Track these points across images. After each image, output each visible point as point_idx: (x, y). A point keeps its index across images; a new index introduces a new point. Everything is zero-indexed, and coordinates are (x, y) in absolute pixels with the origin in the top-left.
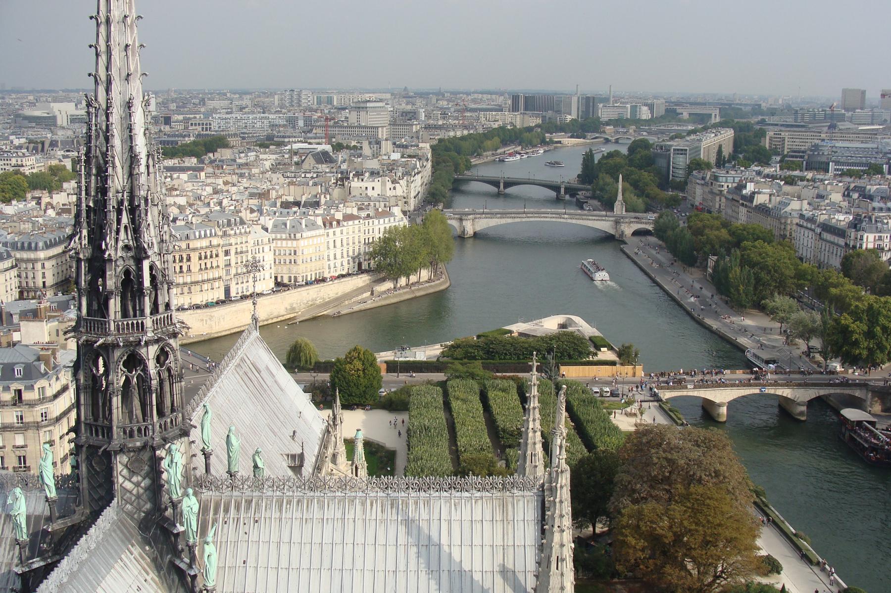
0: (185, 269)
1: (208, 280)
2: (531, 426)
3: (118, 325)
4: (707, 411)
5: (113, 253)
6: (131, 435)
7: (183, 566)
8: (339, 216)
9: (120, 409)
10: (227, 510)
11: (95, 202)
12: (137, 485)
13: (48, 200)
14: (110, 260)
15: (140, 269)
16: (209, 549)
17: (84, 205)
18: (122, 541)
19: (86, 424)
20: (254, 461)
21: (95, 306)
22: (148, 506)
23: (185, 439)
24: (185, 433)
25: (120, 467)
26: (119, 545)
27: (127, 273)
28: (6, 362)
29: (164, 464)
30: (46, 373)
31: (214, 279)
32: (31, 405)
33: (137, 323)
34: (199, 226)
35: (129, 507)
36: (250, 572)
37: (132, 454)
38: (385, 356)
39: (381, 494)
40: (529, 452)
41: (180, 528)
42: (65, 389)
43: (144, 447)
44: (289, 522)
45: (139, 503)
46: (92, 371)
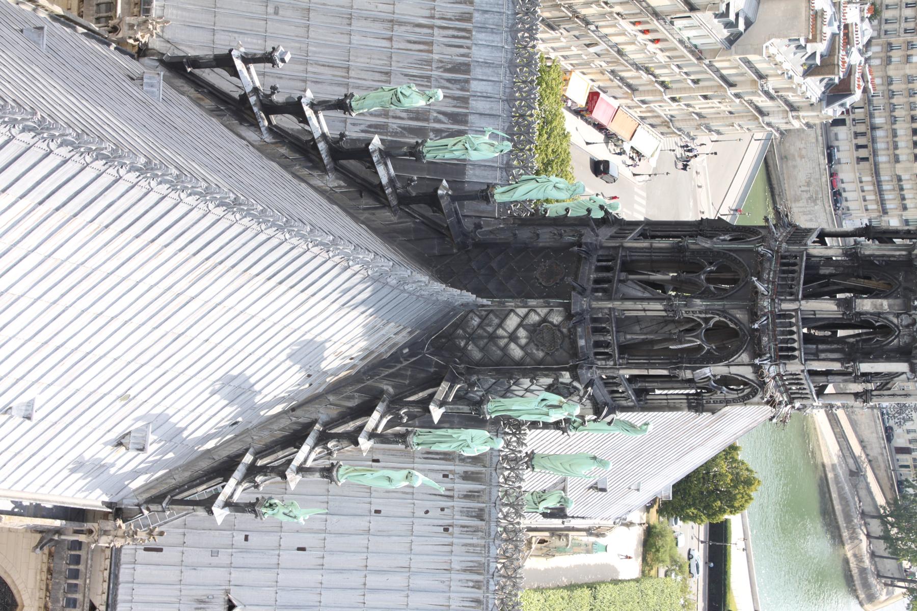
3: (791, 317)
6: (596, 330)
9: (642, 313)
10: (466, 477)
12: (513, 337)
21: (824, 271)
22: (477, 355)
25: (543, 311)
27: (886, 330)
33: (794, 349)
35: (476, 321)
36: (362, 523)
37: (565, 330)
41: (437, 413)
43: (574, 352)
44: (443, 587)
45: (481, 337)
46: (711, 264)
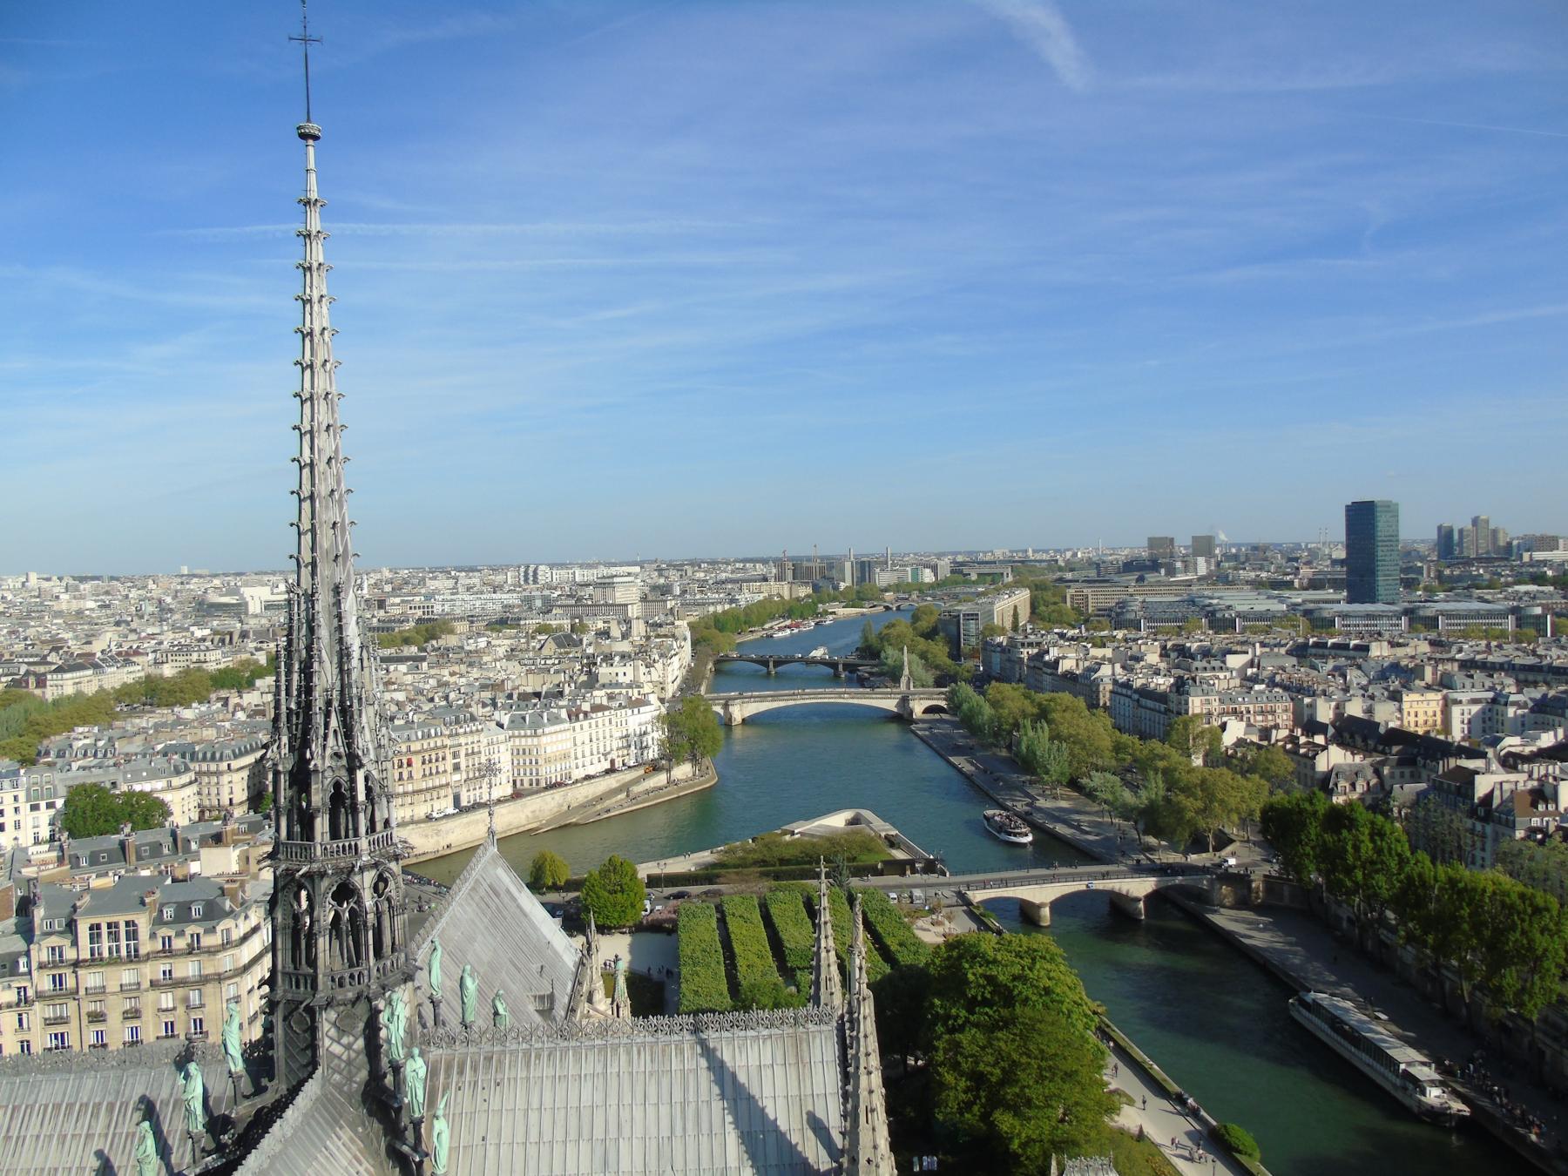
0: (405, 776)
1: (434, 788)
2: (823, 944)
4: (1026, 915)
5: (319, 763)
6: (341, 985)
7: (405, 1149)
8: (586, 707)
10: (461, 1072)
11: (298, 704)
12: (348, 1047)
13: (237, 700)
14: (316, 771)
15: (353, 781)
16: (440, 1125)
17: (283, 708)
18: (328, 1123)
19: (284, 974)
20: (495, 1007)
23: (410, 984)
24: (408, 978)
25: (326, 1026)
26: (323, 1129)
27: (337, 785)
28: (181, 900)
29: (383, 1018)
30: (232, 911)
31: (441, 786)
32: (212, 951)
34: (422, 725)
35: (337, 1077)
36: (491, 1151)
38: (645, 870)
39: (649, 1039)
40: (823, 976)
42: (255, 930)
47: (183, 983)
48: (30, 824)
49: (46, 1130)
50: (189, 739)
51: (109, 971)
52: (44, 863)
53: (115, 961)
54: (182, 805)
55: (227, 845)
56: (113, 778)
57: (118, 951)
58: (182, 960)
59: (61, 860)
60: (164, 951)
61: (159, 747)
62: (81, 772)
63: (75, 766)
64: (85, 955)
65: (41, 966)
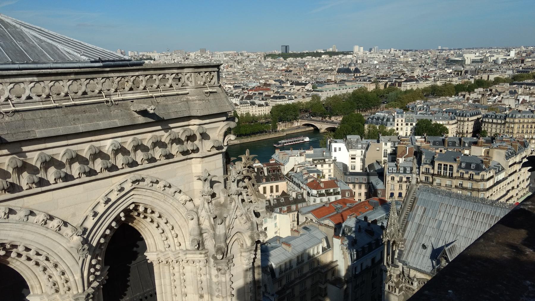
13: (468, 96)
28: (468, 161)
47: (466, 189)
48: (405, 129)
49: (485, 221)
50: (454, 108)
51: (443, 179)
52: (422, 142)
53: (445, 177)
54: (452, 130)
55: (481, 146)
56: (431, 118)
57: (446, 174)
58: (466, 181)
59: (425, 141)
60: (460, 177)
61: (444, 110)
62: (422, 115)
63: (418, 113)
64: (436, 172)
65: (423, 173)
